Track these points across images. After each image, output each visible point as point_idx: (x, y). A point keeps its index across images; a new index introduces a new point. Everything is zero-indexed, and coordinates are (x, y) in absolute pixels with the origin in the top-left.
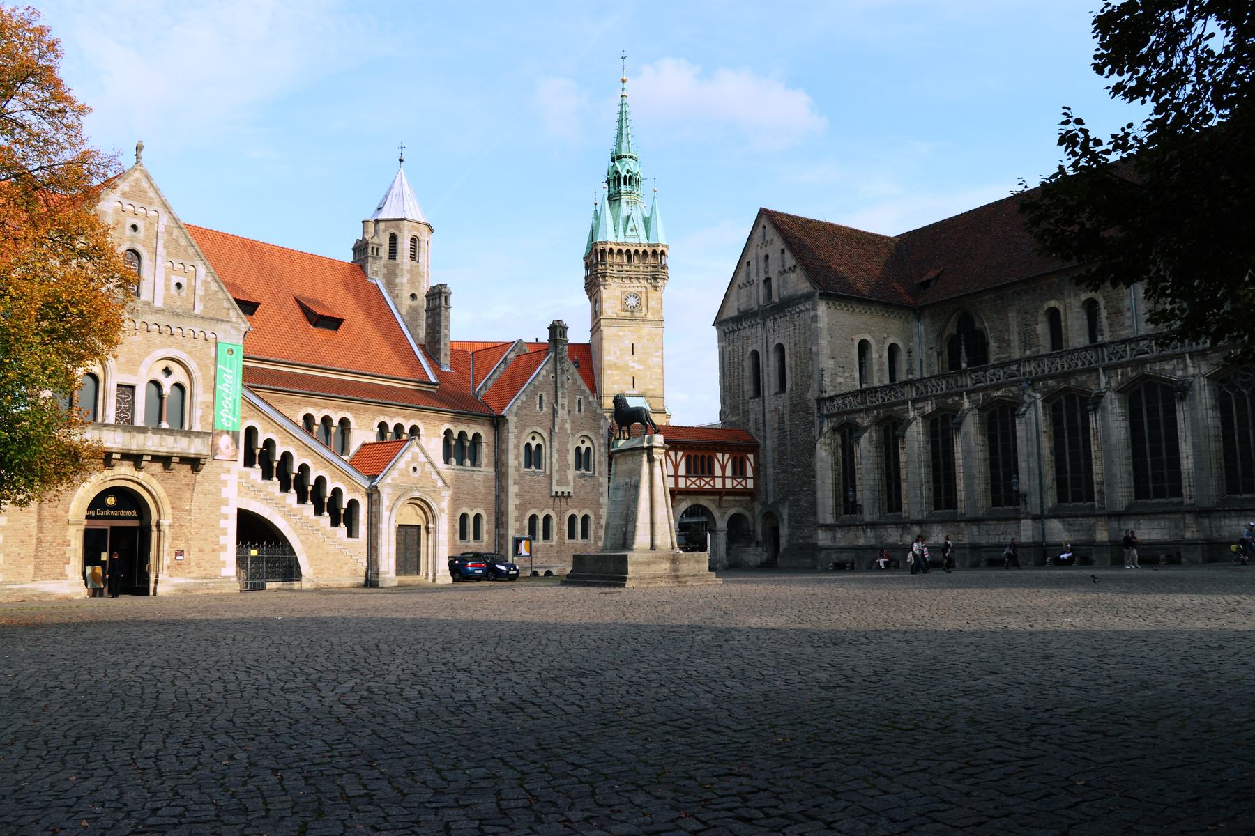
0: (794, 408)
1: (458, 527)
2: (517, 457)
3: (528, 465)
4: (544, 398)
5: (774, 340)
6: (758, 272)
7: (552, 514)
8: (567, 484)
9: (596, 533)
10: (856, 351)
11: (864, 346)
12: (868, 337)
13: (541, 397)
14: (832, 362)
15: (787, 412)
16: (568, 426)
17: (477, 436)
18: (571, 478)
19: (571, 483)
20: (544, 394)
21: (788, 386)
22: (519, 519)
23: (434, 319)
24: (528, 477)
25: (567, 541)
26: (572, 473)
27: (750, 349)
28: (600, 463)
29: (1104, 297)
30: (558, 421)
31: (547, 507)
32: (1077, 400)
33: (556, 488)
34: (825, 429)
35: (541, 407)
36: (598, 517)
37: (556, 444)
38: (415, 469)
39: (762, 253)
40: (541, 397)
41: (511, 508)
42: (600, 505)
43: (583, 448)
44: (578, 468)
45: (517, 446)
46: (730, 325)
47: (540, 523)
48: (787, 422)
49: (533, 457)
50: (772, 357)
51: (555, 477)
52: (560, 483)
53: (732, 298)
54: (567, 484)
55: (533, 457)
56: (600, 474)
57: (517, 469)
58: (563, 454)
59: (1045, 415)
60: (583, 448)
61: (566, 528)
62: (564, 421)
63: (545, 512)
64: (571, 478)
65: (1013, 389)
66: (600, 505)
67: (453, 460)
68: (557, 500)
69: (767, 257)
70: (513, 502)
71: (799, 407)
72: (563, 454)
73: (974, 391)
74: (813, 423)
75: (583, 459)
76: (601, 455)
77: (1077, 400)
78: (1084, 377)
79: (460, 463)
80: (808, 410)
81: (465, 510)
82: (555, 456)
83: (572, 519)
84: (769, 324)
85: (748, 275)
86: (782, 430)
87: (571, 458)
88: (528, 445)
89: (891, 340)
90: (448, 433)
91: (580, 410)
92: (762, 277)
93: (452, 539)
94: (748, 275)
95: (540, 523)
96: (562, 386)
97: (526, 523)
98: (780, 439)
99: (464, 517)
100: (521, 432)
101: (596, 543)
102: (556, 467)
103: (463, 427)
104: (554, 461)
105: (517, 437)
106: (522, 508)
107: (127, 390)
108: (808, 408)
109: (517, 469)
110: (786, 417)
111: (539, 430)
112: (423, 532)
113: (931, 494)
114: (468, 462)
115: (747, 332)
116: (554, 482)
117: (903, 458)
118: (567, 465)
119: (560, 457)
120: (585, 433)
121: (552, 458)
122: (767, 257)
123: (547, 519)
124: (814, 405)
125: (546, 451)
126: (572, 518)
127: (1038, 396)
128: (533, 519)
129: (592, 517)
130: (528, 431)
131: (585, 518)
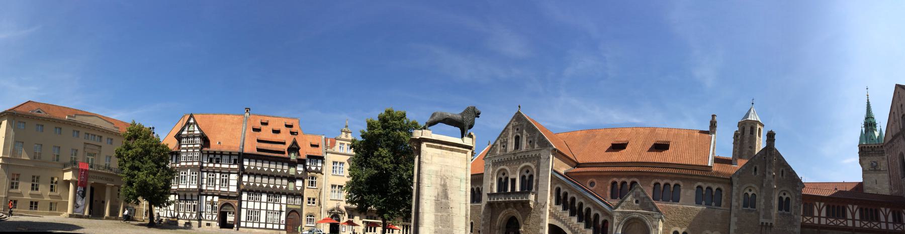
2: (737, 200)
3: (745, 205)
8: (771, 218)
19: (774, 218)
26: (775, 211)
33: (762, 220)
43: (784, 198)
44: (780, 208)
45: (738, 194)
49: (749, 202)
51: (762, 213)
52: (764, 217)
57: (737, 207)
58: (768, 199)
60: (784, 198)
87: (776, 202)
103: (710, 185)
107: (514, 181)
118: (771, 207)
120: (785, 189)
121: (761, 203)
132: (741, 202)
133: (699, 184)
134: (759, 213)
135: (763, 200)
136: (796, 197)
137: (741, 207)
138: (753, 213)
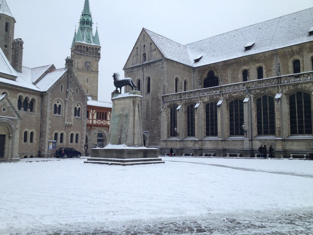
0: (153, 99)
1: (23, 137)
2: (51, 109)
3: (55, 113)
4: (63, 87)
5: (146, 75)
6: (141, 51)
7: (64, 133)
8: (71, 121)
9: (81, 140)
10: (175, 81)
11: (177, 80)
12: (179, 76)
13: (62, 86)
14: (167, 83)
15: (150, 101)
16: (72, 98)
17: (33, 100)
18: (72, 119)
19: (73, 121)
20: (63, 85)
21: (151, 91)
22: (51, 134)
23: (15, 53)
24: (55, 117)
25: (70, 144)
26: (73, 117)
27: (137, 78)
28: (84, 114)
29: (265, 65)
30: (68, 96)
31: (62, 130)
32: (268, 97)
33: (66, 122)
34: (165, 106)
35: (61, 89)
36: (82, 135)
37: (67, 105)
38: (4, 109)
39: (143, 44)
40: (62, 86)
41: (47, 129)
42: (83, 130)
44: (75, 115)
45: (51, 105)
46: (130, 70)
47: (59, 136)
48: (150, 104)
49: (57, 110)
50: (145, 81)
51: (66, 118)
52: (68, 121)
53: (131, 60)
54: (71, 121)
55: (57, 110)
56: (84, 118)
57: (51, 114)
58: (70, 109)
59: (254, 103)
61: (69, 138)
62: (71, 97)
63: (61, 132)
64: (72, 119)
65: (241, 93)
66: (83, 130)
67: (22, 109)
68: (66, 127)
69: (144, 46)
70: (48, 127)
71: (155, 99)
72: (70, 109)
73: (225, 94)
74: (160, 104)
75: (77, 112)
76: (84, 111)
77: (268, 97)
78: (272, 89)
79: (25, 110)
80: (158, 100)
81: (26, 130)
82: (67, 110)
83: (72, 135)
84: (145, 69)
85: (137, 52)
86: (148, 106)
87: (73, 111)
88: (55, 105)
89: (185, 78)
90: (20, 98)
91: (77, 93)
92: (143, 53)
93: (20, 142)
94: (137, 52)
95: (59, 136)
96: (70, 83)
97: (53, 136)
98: (147, 110)
99: (26, 133)
100: (53, 99)
101: (81, 144)
102: (67, 114)
103: (27, 95)
104: (66, 112)
105: (51, 101)
106: (52, 130)
108: (158, 99)
109: (51, 114)
110: (150, 102)
111: (60, 99)
112: (7, 138)
113: (205, 130)
114: (29, 110)
115: (136, 72)
116: (66, 120)
117: (196, 117)
119: (68, 110)
120: (79, 102)
121: (65, 111)
122: (144, 46)
123: (62, 135)
124: (161, 99)
125: (63, 108)
126: (72, 135)
127: (252, 96)
128: (56, 134)
129: (80, 134)
130: (56, 99)
131: (77, 135)
132: (53, 110)
133: (21, 94)
134: (64, 118)
135: (67, 110)
136: (84, 108)
137: (53, 114)
138: (60, 118)
